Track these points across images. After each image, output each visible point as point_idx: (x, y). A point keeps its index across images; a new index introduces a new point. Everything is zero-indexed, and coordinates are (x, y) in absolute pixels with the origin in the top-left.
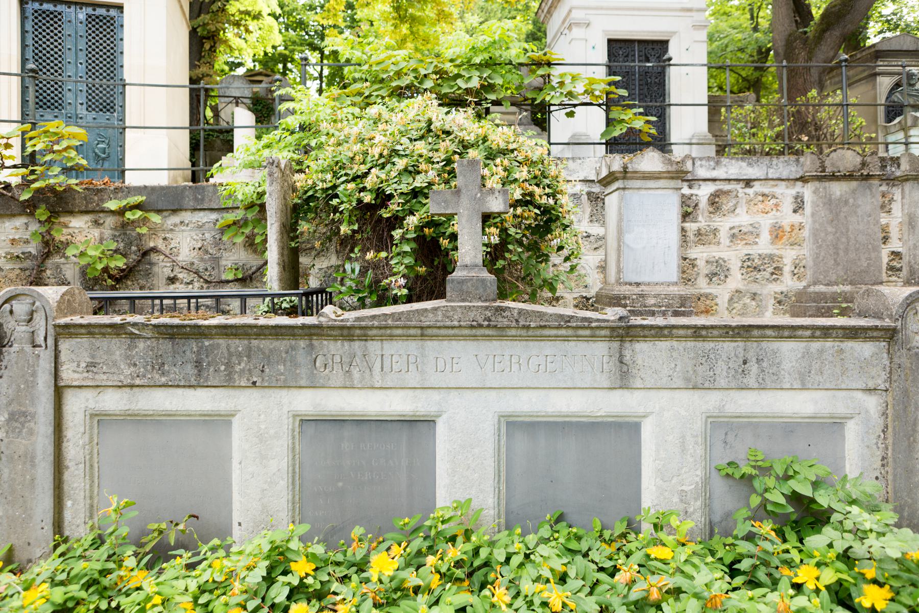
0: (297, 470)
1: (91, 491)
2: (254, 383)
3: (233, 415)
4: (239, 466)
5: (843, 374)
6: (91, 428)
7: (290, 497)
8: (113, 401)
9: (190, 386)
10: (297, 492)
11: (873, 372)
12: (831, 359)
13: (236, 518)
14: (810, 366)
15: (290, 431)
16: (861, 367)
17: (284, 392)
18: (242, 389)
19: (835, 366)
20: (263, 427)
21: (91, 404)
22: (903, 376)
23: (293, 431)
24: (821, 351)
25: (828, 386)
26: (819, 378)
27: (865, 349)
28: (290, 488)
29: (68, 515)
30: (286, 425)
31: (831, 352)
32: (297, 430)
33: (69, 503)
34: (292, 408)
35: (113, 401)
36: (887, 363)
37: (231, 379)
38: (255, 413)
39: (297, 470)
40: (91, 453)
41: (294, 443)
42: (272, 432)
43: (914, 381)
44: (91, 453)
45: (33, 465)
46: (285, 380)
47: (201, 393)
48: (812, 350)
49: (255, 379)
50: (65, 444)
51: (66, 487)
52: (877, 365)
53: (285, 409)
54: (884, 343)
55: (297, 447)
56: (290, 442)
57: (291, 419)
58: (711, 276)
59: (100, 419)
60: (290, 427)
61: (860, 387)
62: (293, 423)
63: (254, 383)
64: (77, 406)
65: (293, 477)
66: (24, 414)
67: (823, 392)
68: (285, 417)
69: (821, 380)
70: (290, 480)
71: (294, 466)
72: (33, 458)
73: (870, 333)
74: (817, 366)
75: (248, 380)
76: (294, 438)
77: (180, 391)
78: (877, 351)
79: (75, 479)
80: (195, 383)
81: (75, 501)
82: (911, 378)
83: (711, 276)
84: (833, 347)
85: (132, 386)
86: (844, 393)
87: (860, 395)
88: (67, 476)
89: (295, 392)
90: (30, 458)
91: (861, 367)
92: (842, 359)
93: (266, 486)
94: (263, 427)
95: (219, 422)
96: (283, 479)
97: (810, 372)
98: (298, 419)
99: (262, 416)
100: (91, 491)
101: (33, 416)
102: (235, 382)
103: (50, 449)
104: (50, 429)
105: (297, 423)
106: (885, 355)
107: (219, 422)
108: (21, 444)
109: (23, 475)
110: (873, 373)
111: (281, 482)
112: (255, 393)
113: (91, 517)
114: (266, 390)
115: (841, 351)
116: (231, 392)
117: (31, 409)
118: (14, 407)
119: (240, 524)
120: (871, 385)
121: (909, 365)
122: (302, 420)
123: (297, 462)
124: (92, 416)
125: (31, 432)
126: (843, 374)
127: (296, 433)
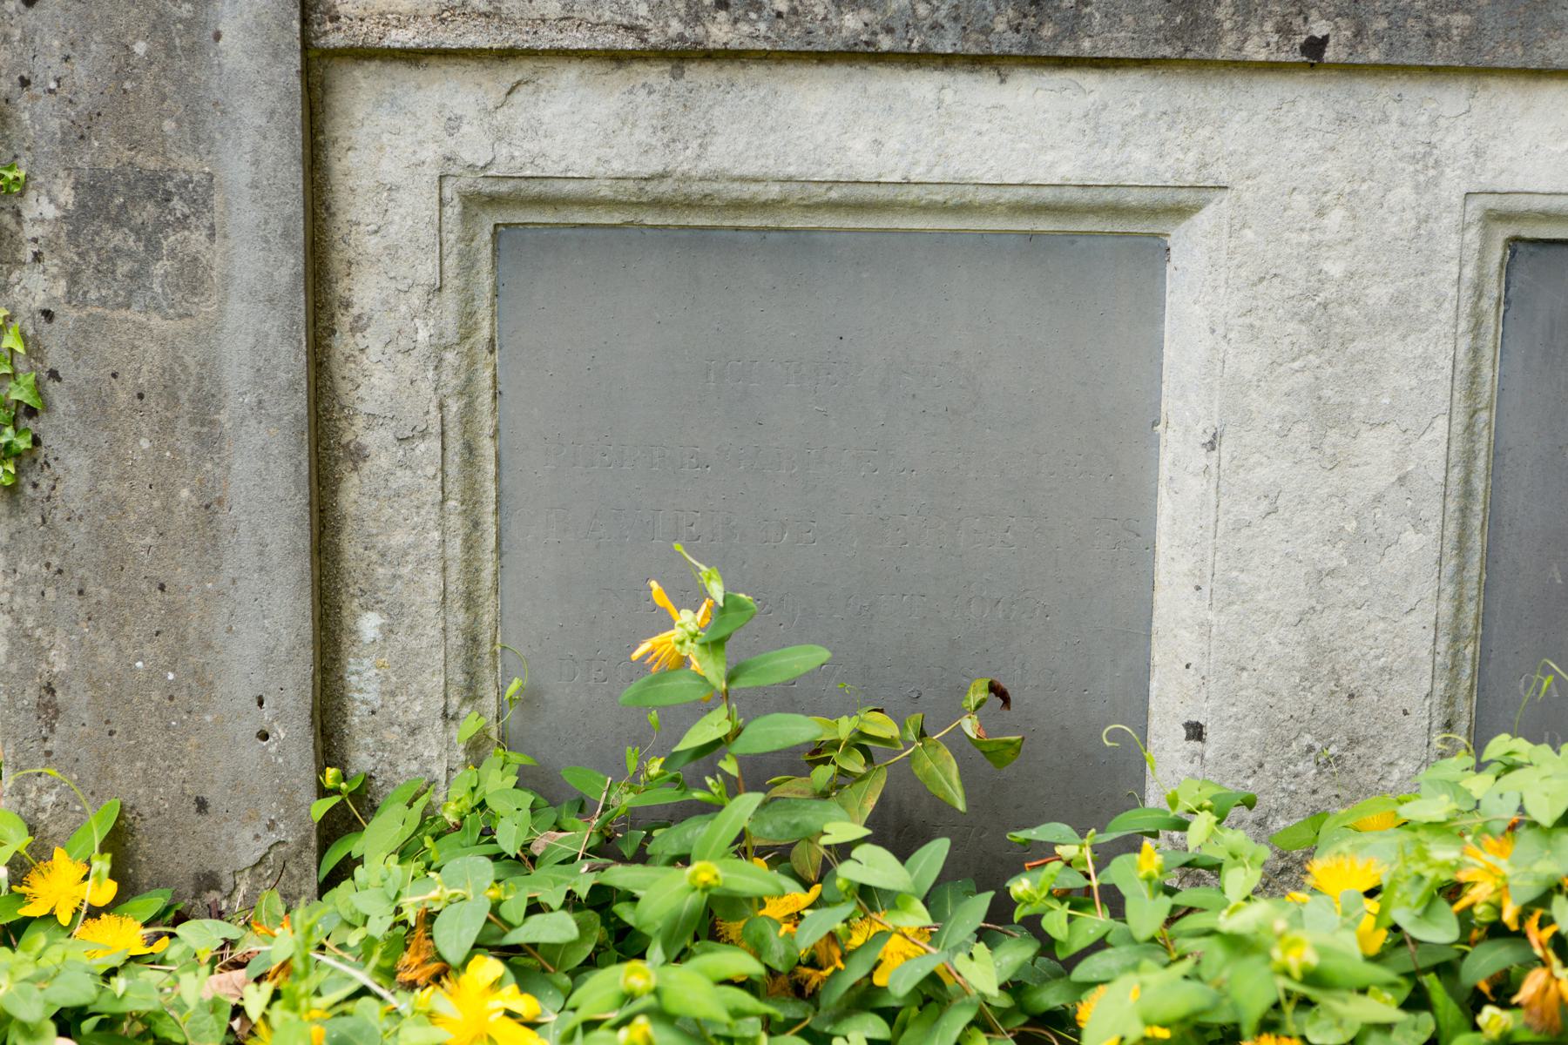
0: (1479, 485)
1: (471, 570)
2: (1315, 47)
3: (1181, 212)
4: (1201, 458)
6: (468, 264)
7: (1446, 608)
8: (582, 132)
9: (977, 62)
10: (1472, 589)
13: (1170, 699)
15: (1467, 293)
17: (1451, 99)
18: (1239, 81)
20: (1335, 269)
21: (474, 147)
23: (1479, 290)
28: (1450, 565)
29: (364, 680)
30: (1458, 261)
32: (1494, 289)
33: (369, 625)
34: (1485, 180)
35: (582, 132)
37: (1195, 23)
38: (1300, 201)
39: (1479, 485)
40: (467, 390)
41: (1475, 353)
42: (1379, 294)
44: (467, 390)
45: (209, 440)
46: (1471, 38)
47: (1032, 98)
49: (1319, 28)
50: (343, 343)
51: (351, 548)
53: (1453, 184)
55: (1487, 371)
56: (1464, 344)
57: (1473, 235)
59: (514, 223)
60: (1469, 272)
62: (1483, 252)
63: (1315, 47)
64: (400, 146)
65: (1464, 511)
66: (156, 187)
68: (1448, 220)
70: (1452, 528)
71: (1469, 458)
72: (206, 405)
75: (1285, 30)
76: (1477, 328)
77: (923, 85)
79: (402, 511)
80: (1005, 39)
81: (395, 614)
85: (680, 56)
88: (353, 494)
89: (1505, 98)
90: (190, 405)
93: (1334, 557)
94: (1335, 269)
95: (1106, 245)
96: (1418, 524)
98: (1504, 232)
99: (1336, 217)
100: (471, 570)
101: (201, 196)
102: (1215, 40)
103: (292, 361)
104: (289, 266)
105: (1497, 254)
107: (1106, 245)
108: (147, 333)
109: (165, 488)
111: (1410, 537)
112: (1306, 103)
113: (471, 693)
114: (1364, 87)
116: (1186, 93)
117: (189, 164)
118: (106, 153)
119: (1195, 731)
122: (1514, 243)
123: (1482, 445)
124: (475, 202)
125: (192, 277)
127: (1487, 304)
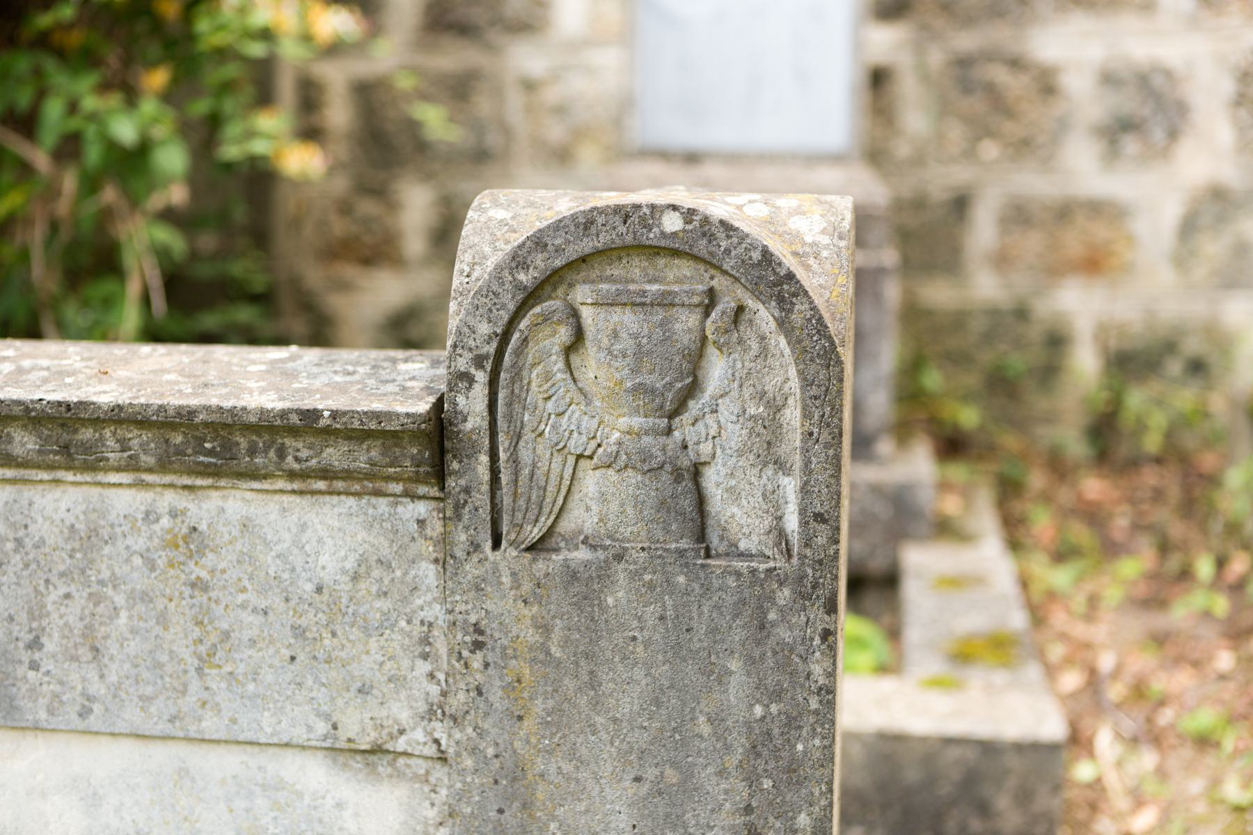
5: (205, 661)
11: (368, 660)
12: (139, 579)
14: (37, 612)
16: (299, 632)
19: (163, 619)
22: (495, 695)
24: (88, 538)
25: (132, 716)
26: (84, 677)
27: (322, 536)
31: (139, 543)
36: (436, 612)
43: (555, 721)
48: (41, 528)
52: (386, 623)
54: (422, 508)
58: (1117, 131)
61: (299, 734)
67: (128, 745)
69: (97, 688)
73: (300, 450)
74: (73, 612)
78: (386, 551)
82: (539, 706)
83: (1117, 131)
84: (150, 516)
86: (228, 762)
87: (313, 775)
91: (299, 632)
92: (198, 585)
97: (35, 644)
106: (428, 573)
110: (366, 667)
115: (192, 541)
120: (356, 724)
121: (531, 636)
126: (205, 661)
